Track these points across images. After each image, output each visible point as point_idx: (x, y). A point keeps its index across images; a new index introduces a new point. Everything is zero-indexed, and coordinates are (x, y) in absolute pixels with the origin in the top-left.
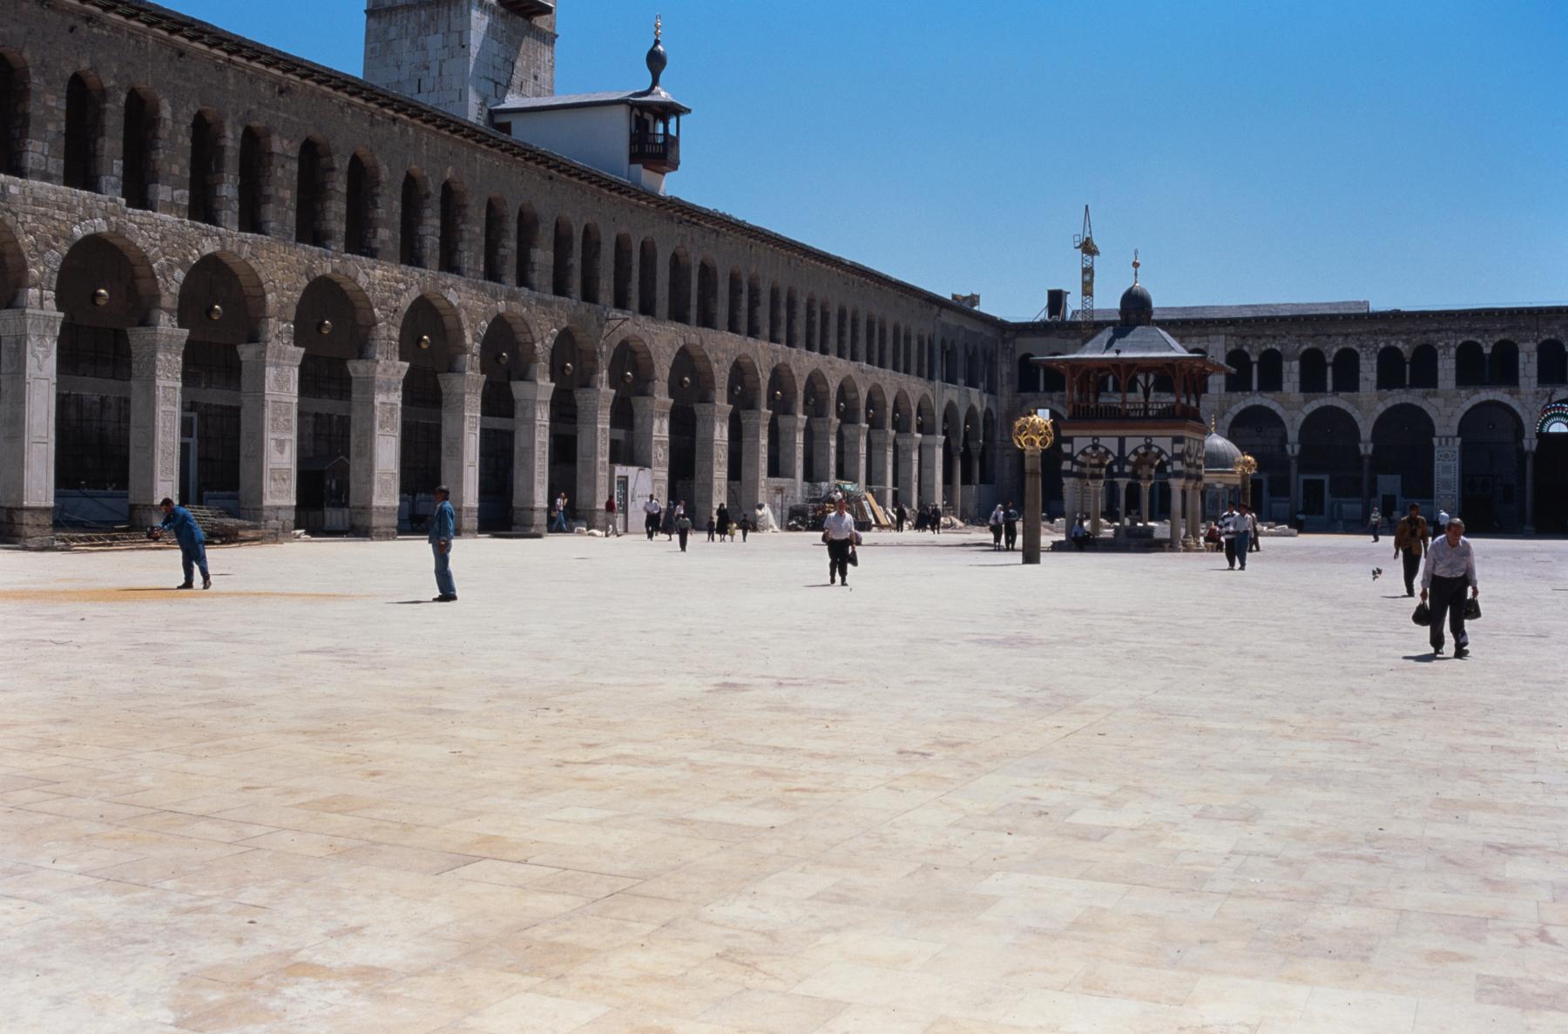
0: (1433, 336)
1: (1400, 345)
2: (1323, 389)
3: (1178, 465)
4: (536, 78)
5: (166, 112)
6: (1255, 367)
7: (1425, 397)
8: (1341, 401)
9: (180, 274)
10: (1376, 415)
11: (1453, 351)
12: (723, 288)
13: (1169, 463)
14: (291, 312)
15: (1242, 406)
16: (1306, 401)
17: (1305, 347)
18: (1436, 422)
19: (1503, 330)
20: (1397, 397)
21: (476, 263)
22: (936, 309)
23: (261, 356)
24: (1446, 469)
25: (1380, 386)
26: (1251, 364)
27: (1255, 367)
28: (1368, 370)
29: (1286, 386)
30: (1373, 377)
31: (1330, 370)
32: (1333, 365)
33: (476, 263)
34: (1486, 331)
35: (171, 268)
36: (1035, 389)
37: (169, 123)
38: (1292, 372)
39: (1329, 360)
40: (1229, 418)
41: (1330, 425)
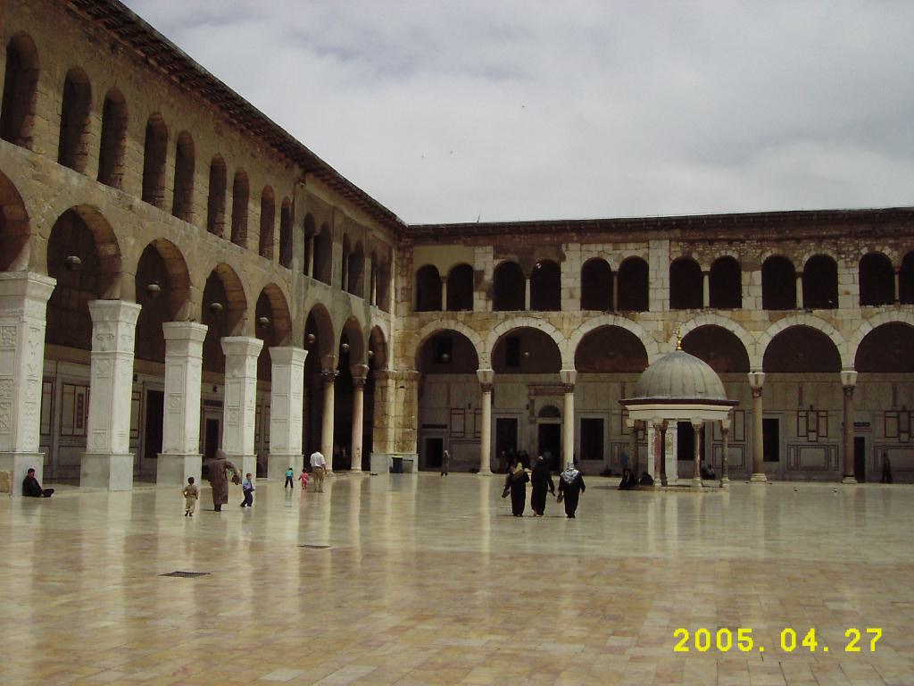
1: (887, 251)
6: (706, 279)
8: (816, 320)
10: (861, 338)
15: (692, 326)
16: (772, 320)
17: (768, 254)
22: (297, 171)
26: (701, 275)
27: (706, 279)
28: (849, 281)
29: (747, 302)
30: (855, 289)
31: (799, 283)
32: (803, 276)
36: (437, 307)
38: (752, 285)
39: (799, 269)
41: (802, 353)
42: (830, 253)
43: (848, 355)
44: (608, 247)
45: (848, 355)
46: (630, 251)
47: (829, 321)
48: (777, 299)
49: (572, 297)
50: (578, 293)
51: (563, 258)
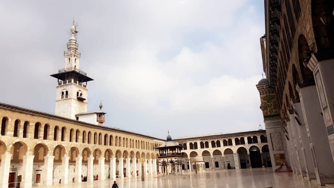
0: (231, 137)
1: (226, 139)
2: (215, 147)
3: (176, 163)
4: (84, 109)
5: (10, 120)
7: (231, 147)
8: (218, 149)
9: (11, 146)
11: (234, 140)
12: (114, 139)
13: (175, 162)
14: (33, 150)
18: (233, 151)
19: (241, 136)
20: (227, 147)
21: (68, 139)
23: (26, 158)
24: (236, 158)
25: (224, 146)
28: (222, 143)
29: (209, 147)
32: (216, 143)
33: (68, 139)
34: (239, 136)
35: (10, 144)
37: (10, 122)
38: (210, 145)
39: (215, 142)
40: (202, 153)
41: (217, 153)
42: (219, 140)
43: (223, 153)
44: (192, 141)
45: (223, 153)
46: (195, 141)
47: (220, 149)
48: (213, 146)
49: (188, 148)
50: (189, 147)
51: (187, 143)
